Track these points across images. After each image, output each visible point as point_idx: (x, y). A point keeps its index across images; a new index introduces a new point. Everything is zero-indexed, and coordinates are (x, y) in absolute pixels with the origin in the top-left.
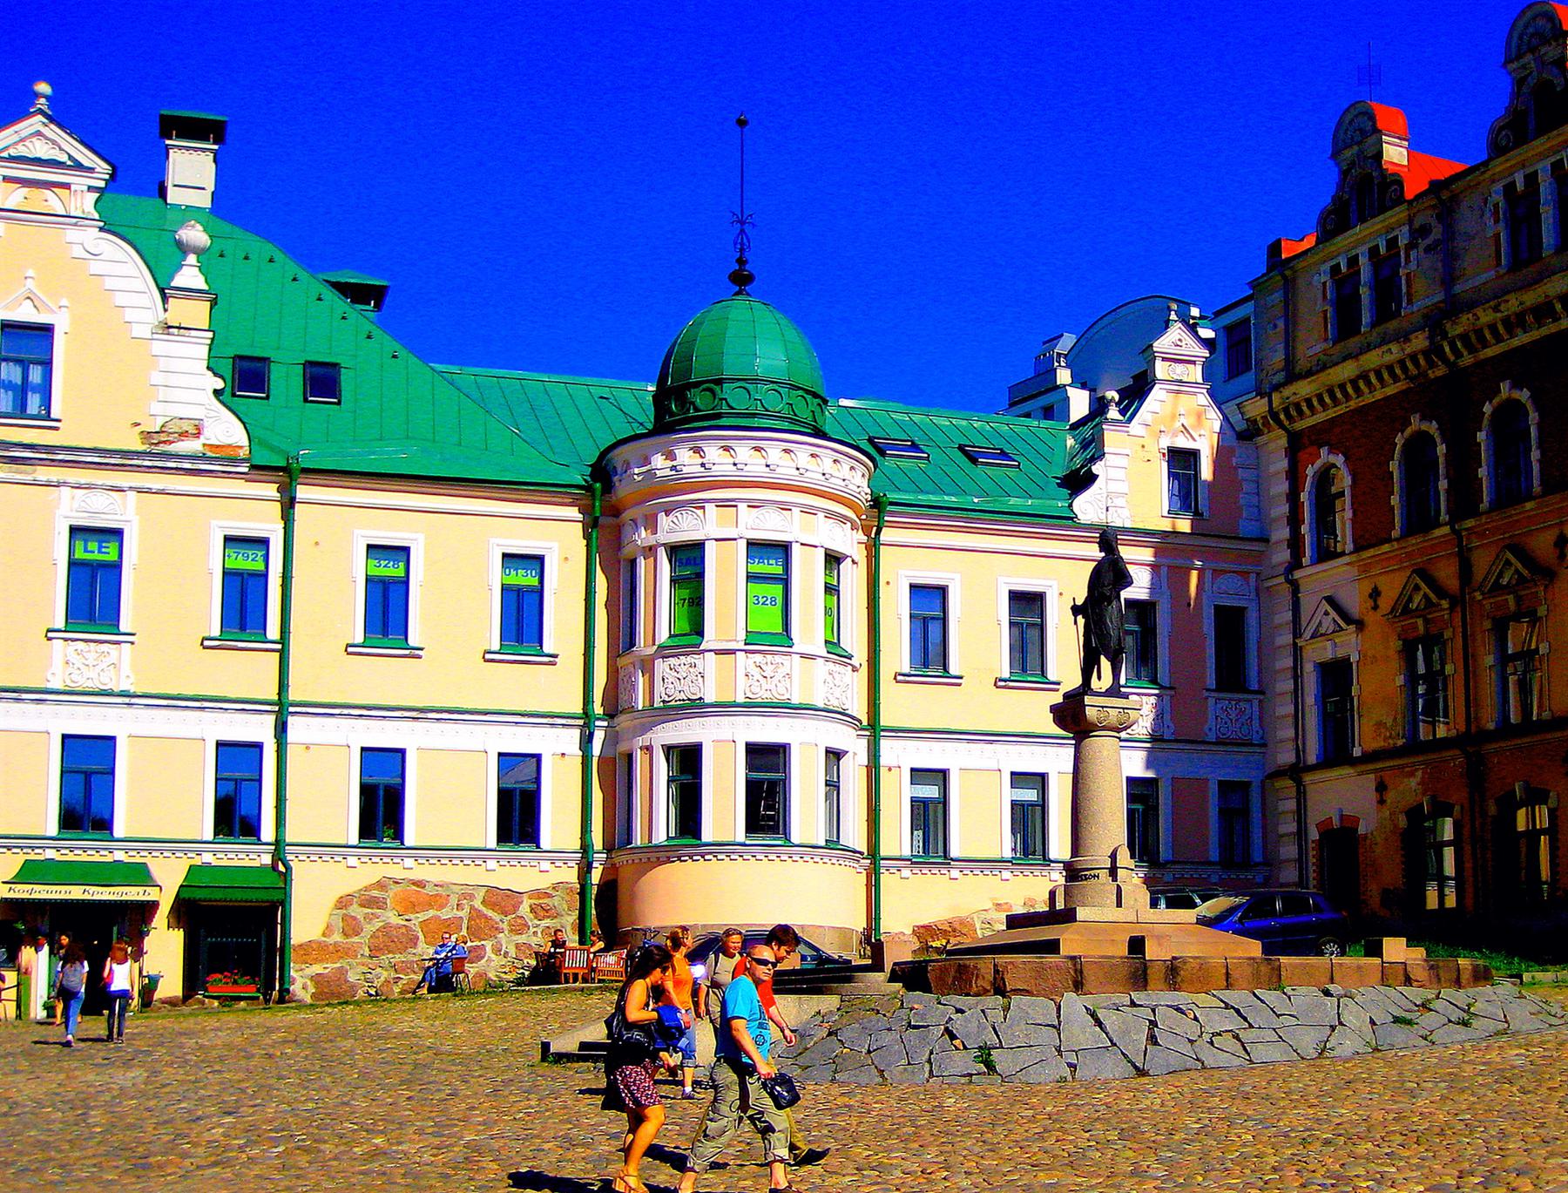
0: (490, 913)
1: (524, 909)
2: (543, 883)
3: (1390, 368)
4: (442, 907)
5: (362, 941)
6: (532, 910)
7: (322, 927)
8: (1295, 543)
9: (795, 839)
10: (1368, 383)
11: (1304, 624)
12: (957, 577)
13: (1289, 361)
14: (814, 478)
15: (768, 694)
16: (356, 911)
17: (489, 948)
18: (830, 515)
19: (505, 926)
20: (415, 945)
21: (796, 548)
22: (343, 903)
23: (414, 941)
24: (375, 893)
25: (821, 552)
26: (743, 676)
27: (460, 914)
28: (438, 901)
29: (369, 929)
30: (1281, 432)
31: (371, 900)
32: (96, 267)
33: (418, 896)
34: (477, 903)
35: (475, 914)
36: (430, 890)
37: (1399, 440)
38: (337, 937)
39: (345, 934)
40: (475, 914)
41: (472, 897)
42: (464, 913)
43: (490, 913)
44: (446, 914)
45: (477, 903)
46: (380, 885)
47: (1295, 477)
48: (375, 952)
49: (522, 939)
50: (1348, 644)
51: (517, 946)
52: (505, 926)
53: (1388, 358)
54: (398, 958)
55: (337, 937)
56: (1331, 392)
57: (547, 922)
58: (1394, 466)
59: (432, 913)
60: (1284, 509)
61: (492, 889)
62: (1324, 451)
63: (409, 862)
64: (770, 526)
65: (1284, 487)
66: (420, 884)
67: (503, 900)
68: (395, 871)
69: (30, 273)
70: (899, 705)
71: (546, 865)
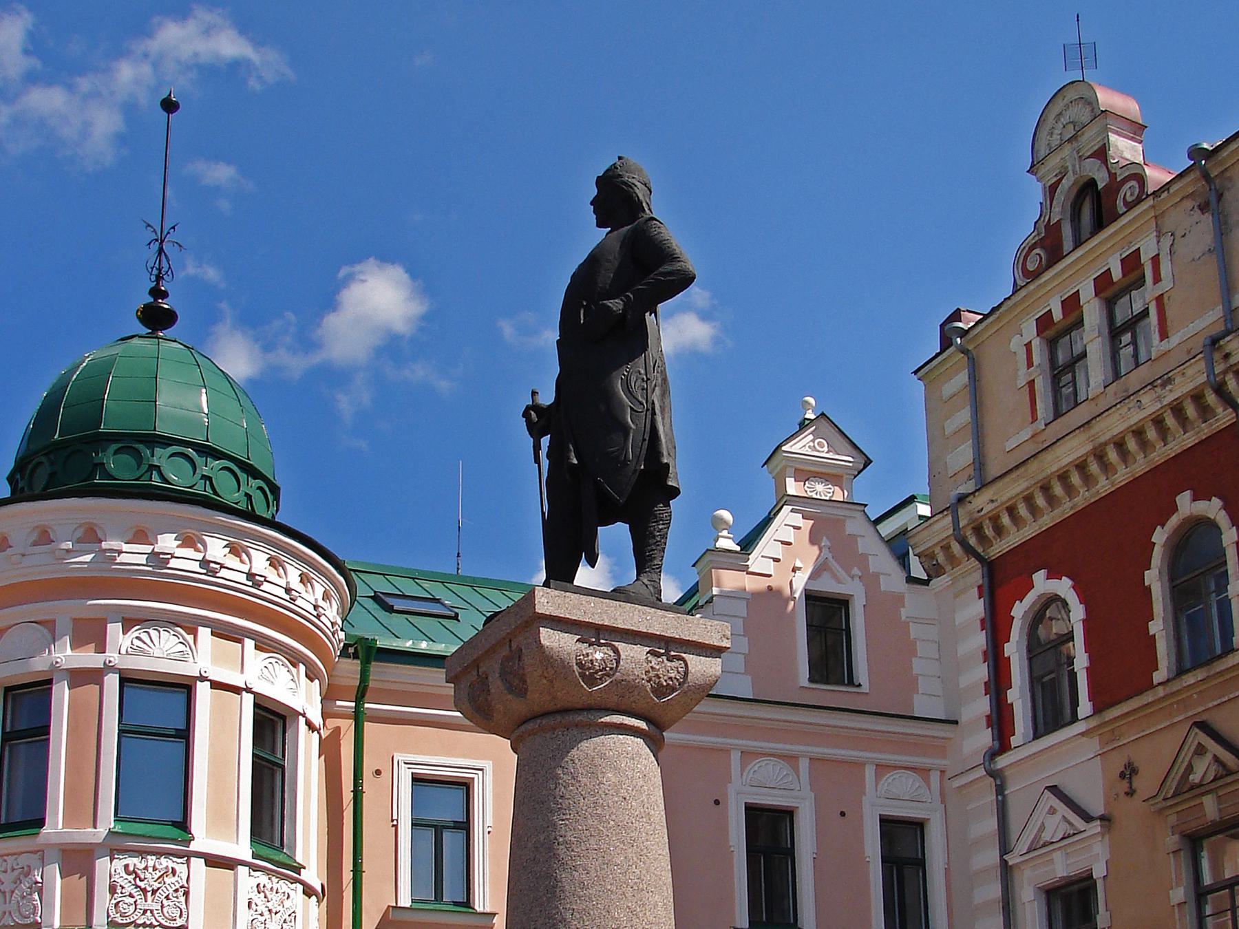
3: (1139, 433)
8: (1001, 721)
10: (1106, 467)
11: (1013, 836)
13: (980, 462)
21: (203, 689)
25: (248, 699)
30: (974, 562)
37: (1160, 537)
47: (996, 626)
50: (1094, 856)
53: (1135, 417)
56: (1046, 489)
58: (1154, 578)
60: (981, 672)
62: (1039, 577)
64: (161, 652)
65: (980, 640)
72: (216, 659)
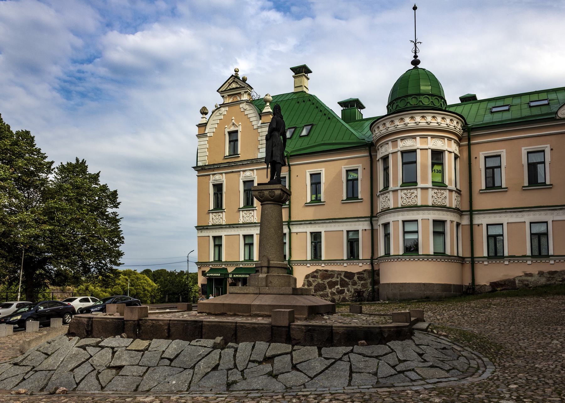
0: (346, 279)
1: (356, 278)
2: (360, 270)
4: (332, 278)
5: (312, 287)
6: (358, 278)
7: (302, 283)
9: (420, 253)
12: (504, 150)
14: (434, 124)
15: (409, 204)
16: (311, 279)
17: (346, 290)
18: (433, 137)
19: (350, 283)
20: (326, 289)
22: (307, 277)
23: (325, 288)
24: (315, 274)
26: (403, 198)
27: (338, 280)
28: (332, 276)
29: (314, 284)
31: (313, 275)
32: (246, 113)
33: (326, 274)
34: (342, 277)
35: (342, 280)
36: (329, 273)
38: (306, 287)
39: (308, 286)
40: (342, 280)
41: (340, 274)
42: (338, 280)
43: (346, 279)
44: (334, 280)
45: (342, 277)
46: (317, 271)
48: (316, 291)
49: (355, 287)
51: (354, 289)
52: (350, 283)
54: (322, 293)
55: (306, 287)
57: (362, 282)
59: (330, 279)
61: (346, 272)
63: (323, 265)
66: (326, 271)
67: (349, 275)
68: (320, 268)
69: (233, 118)
70: (482, 201)
71: (361, 264)
72: (421, 144)
